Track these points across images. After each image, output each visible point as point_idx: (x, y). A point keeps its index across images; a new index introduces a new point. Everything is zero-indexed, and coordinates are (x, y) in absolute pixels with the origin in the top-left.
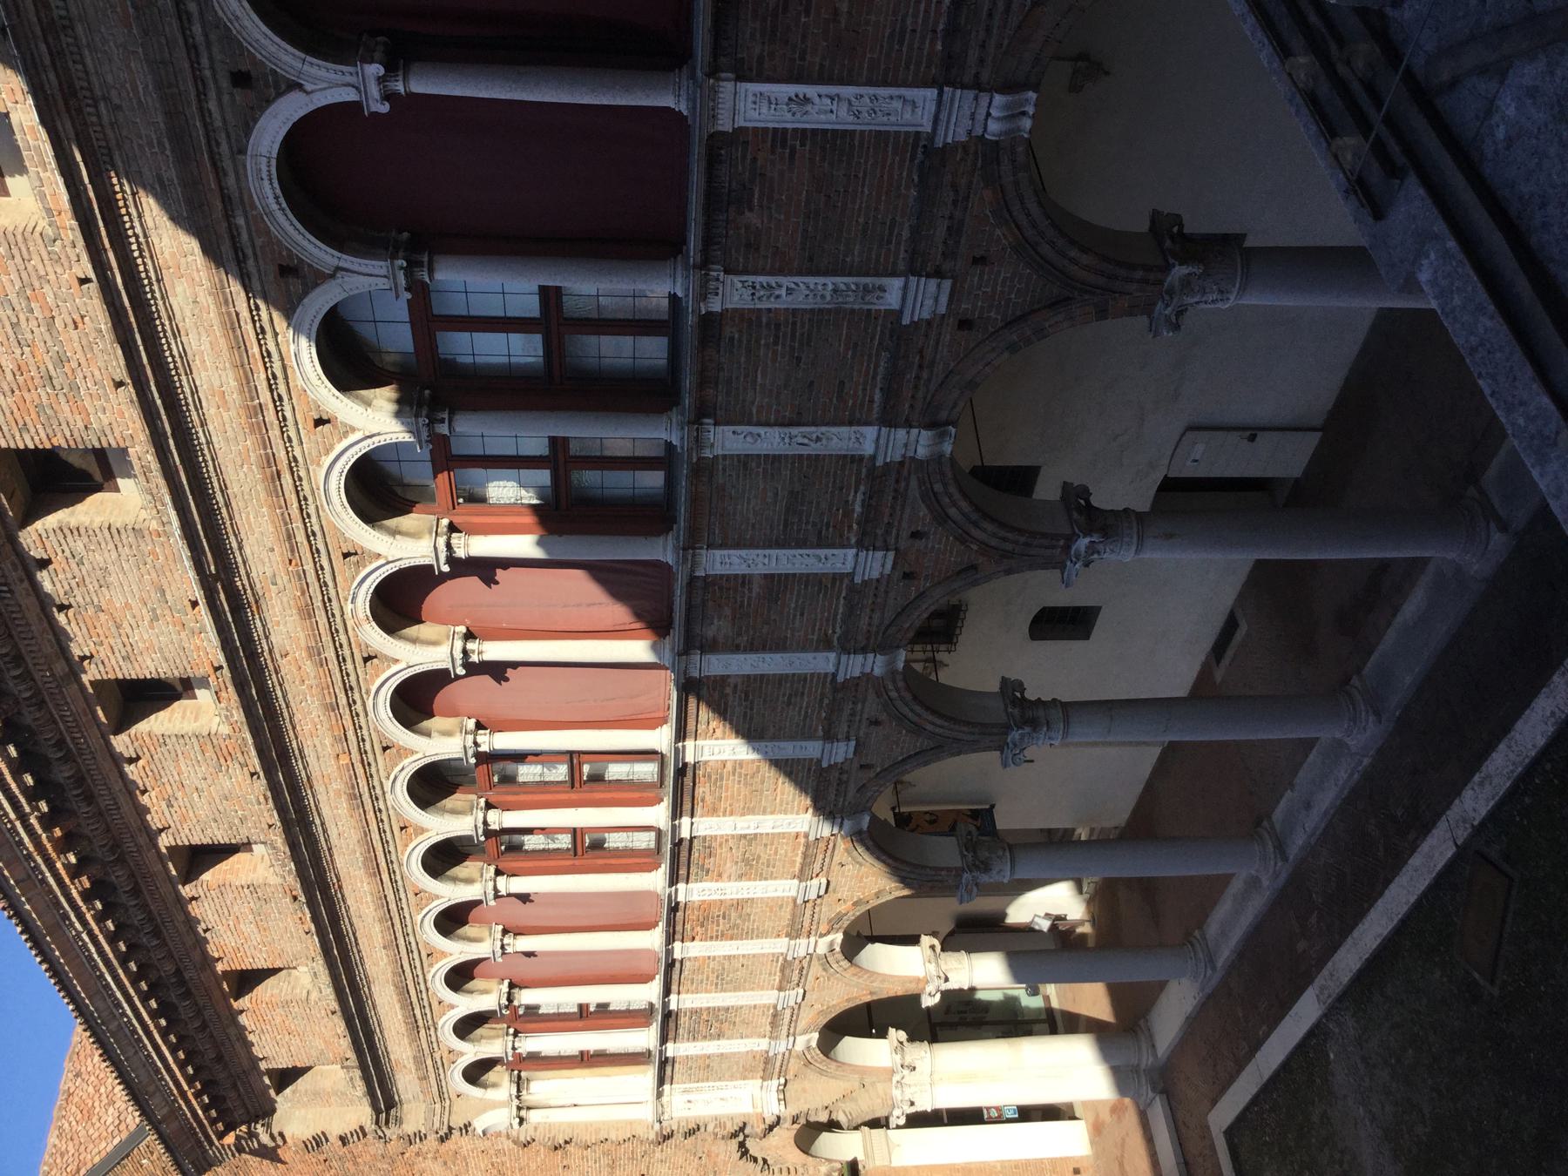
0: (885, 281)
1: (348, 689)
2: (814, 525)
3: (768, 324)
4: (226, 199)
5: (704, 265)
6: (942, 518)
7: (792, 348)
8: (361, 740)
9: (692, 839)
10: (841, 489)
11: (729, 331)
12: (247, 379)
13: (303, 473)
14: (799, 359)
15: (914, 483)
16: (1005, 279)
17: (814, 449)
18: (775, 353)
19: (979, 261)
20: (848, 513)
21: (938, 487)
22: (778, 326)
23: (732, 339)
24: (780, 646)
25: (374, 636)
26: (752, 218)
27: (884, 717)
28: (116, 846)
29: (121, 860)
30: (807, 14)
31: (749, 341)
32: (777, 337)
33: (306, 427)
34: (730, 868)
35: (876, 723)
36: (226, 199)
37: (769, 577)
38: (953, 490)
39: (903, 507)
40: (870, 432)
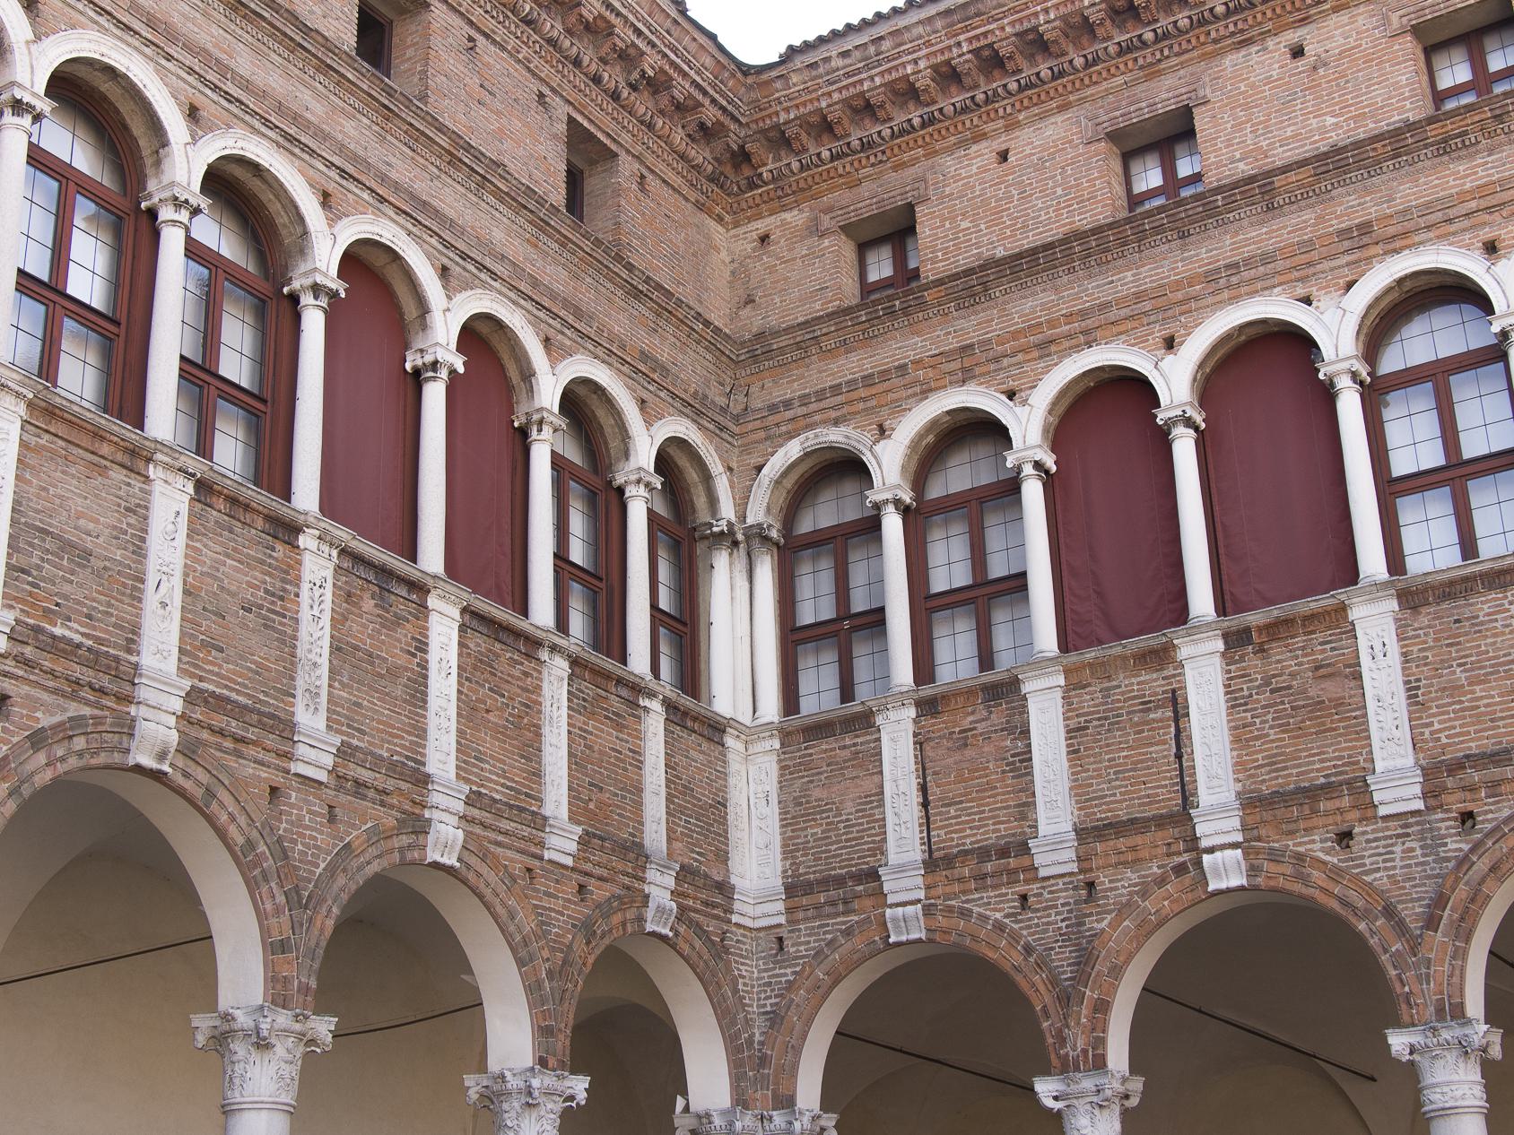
0: (323, 714)
2: (39, 568)
3: (284, 590)
4: (383, 200)
5: (344, 552)
6: (37, 739)
7: (261, 607)
10: (89, 617)
11: (281, 550)
12: (247, 85)
13: (147, 50)
14: (249, 611)
15: (87, 711)
16: (315, 839)
17: (151, 600)
18: (257, 588)
21: (80, 743)
22: (282, 599)
23: (273, 549)
26: (368, 604)
30: (490, 689)
31: (270, 565)
32: (273, 595)
33: (200, 100)
36: (383, 200)
38: (73, 762)
39: (55, 692)
40: (171, 665)
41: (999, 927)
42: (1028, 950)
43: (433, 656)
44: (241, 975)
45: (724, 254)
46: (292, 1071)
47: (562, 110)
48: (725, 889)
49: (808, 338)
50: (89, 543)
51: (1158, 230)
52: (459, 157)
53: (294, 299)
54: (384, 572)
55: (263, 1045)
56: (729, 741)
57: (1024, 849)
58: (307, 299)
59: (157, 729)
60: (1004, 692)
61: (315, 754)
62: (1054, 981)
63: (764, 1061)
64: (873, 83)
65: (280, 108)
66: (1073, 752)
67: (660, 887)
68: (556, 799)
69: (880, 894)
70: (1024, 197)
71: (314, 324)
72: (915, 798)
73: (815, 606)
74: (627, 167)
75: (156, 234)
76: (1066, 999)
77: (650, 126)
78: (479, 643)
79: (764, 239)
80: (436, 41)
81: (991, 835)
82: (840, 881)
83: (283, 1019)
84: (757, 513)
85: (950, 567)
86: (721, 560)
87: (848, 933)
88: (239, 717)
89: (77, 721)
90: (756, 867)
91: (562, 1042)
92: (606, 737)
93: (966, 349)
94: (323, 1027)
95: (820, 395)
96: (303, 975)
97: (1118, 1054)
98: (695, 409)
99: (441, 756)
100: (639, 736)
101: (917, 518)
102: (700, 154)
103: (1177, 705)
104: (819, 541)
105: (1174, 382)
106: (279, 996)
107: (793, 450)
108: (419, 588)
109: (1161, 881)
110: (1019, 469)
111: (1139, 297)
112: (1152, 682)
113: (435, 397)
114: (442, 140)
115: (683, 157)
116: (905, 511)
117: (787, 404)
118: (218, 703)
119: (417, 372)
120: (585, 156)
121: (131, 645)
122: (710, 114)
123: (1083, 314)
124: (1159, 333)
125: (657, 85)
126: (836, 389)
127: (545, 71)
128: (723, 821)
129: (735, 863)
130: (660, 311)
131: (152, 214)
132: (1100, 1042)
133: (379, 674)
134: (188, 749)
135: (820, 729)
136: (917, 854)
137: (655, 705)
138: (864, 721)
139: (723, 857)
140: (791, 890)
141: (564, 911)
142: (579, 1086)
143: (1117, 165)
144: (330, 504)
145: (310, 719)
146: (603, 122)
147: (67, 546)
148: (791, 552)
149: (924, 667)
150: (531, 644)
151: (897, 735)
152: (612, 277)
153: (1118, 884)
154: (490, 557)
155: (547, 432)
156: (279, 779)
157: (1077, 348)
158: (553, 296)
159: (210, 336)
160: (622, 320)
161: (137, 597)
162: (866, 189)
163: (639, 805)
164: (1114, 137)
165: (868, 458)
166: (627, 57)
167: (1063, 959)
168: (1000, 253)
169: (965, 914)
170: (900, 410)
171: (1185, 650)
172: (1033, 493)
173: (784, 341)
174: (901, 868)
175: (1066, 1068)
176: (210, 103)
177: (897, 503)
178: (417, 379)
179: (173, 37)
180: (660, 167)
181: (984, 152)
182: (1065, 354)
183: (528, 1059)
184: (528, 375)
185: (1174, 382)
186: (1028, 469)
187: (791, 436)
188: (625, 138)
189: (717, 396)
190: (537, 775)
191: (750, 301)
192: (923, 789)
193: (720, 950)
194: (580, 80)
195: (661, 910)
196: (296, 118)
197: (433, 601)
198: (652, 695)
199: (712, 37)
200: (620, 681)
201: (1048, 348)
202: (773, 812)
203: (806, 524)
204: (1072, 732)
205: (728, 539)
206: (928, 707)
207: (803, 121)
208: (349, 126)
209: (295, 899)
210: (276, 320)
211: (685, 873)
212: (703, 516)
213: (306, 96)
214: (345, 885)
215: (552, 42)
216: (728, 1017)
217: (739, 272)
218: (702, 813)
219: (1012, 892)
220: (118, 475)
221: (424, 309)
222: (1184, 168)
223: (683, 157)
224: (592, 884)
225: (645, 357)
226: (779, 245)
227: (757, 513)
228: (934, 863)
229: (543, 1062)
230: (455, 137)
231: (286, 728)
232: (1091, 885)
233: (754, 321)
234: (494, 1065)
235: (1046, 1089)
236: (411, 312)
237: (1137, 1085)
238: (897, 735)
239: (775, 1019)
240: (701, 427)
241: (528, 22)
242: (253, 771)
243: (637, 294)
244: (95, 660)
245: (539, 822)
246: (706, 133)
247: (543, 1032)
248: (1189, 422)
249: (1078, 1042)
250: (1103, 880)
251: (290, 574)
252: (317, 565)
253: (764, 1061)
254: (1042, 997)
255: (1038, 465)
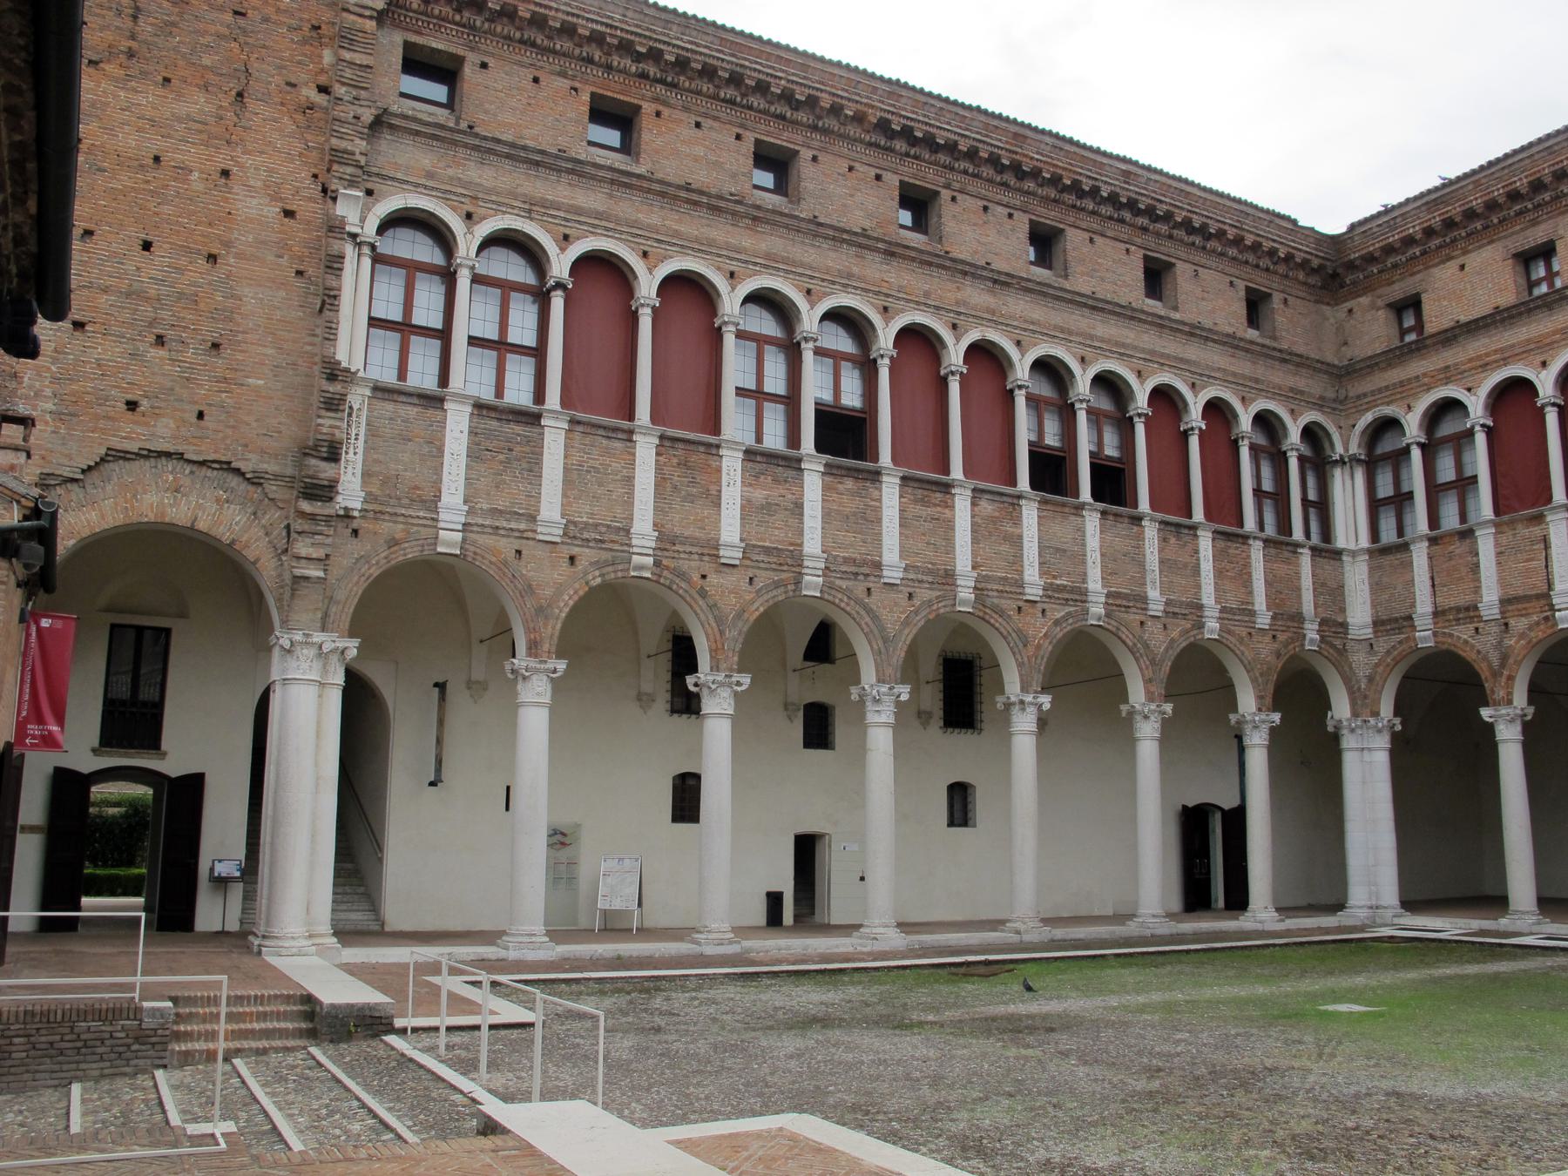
1: (937, 308)
5: (1161, 522)
6: (1057, 623)
8: (899, 299)
9: (801, 470)
19: (1165, 627)
20: (1055, 577)
24: (975, 541)
25: (973, 336)
26: (1173, 540)
27: (917, 602)
28: (826, 131)
29: (815, 128)
34: (759, 495)
35: (910, 596)
37: (1020, 537)
41: (1466, 642)
42: (1479, 652)
43: (1201, 555)
44: (1137, 693)
45: (1332, 320)
46: (1157, 725)
47: (1241, 285)
48: (1344, 625)
49: (1374, 364)
50: (1065, 547)
51: (1536, 308)
52: (1194, 332)
53: (1131, 418)
54: (1178, 525)
55: (1146, 717)
56: (1345, 558)
57: (1476, 608)
58: (1136, 419)
59: (1097, 609)
60: (1467, 534)
61: (1156, 606)
62: (1490, 666)
63: (1366, 697)
64: (1394, 238)
65: (1117, 344)
66: (1499, 563)
67: (1312, 633)
68: (1260, 602)
69: (1413, 627)
70: (1473, 290)
71: (1140, 430)
72: (1428, 583)
73: (1385, 489)
74: (1277, 298)
75: (1075, 414)
76: (1496, 674)
77: (1286, 276)
78: (1221, 544)
79: (1350, 311)
80: (1180, 280)
81: (1463, 600)
82: (1396, 620)
83: (1153, 707)
84: (1354, 448)
85: (1446, 470)
86: (1337, 472)
87: (1400, 642)
88: (1126, 600)
89: (1069, 614)
90: (1359, 614)
91: (1269, 700)
92: (1281, 569)
93: (1447, 367)
94: (1168, 708)
95: (1380, 390)
96: (1159, 690)
97: (1520, 698)
98: (1320, 404)
99: (1208, 596)
100: (1298, 565)
101: (1429, 450)
102: (1312, 280)
103: (1546, 541)
104: (1386, 457)
105: (1546, 385)
106: (1150, 698)
107: (1369, 417)
108: (1194, 528)
109: (1538, 624)
110: (1473, 427)
111: (1528, 341)
112: (1536, 531)
113: (1194, 442)
114: (1187, 329)
115: (1305, 284)
116: (1422, 446)
117: (1365, 395)
118: (1117, 595)
119: (1186, 432)
120: (1255, 305)
121: (1084, 581)
122: (1315, 263)
123: (1501, 350)
124: (1540, 359)
125: (1289, 258)
126: (1387, 388)
127: (1232, 271)
128: (1343, 594)
129: (1348, 612)
130: (1298, 365)
131: (1072, 405)
132: (1510, 694)
133: (1181, 568)
134: (1108, 615)
135: (1386, 550)
136: (1429, 609)
137: (1306, 551)
138: (1404, 547)
139: (1343, 610)
140: (1377, 624)
141: (1265, 649)
142: (1276, 717)
143: (1520, 269)
144: (1153, 506)
145: (1153, 593)
146: (1261, 282)
147: (1058, 550)
148: (1371, 465)
149: (1434, 522)
150: (1245, 538)
151: (1420, 555)
152: (1273, 358)
153: (1519, 624)
154: (1224, 506)
155: (1246, 442)
156: (1143, 618)
157: (1499, 367)
158: (1244, 377)
159: (1100, 443)
160: (1280, 377)
161: (1084, 562)
162: (1396, 287)
163: (1299, 597)
164: (1517, 256)
165: (1403, 421)
166: (1272, 253)
167: (1495, 659)
168: (1463, 319)
169: (1451, 635)
170: (1415, 396)
171: (1549, 519)
172: (1480, 439)
173: (1362, 365)
174: (1423, 615)
175: (1496, 704)
176: (1088, 352)
177: (1419, 444)
178: (1185, 435)
179: (1070, 333)
180: (1294, 292)
181: (1452, 266)
182: (1494, 370)
183: (1254, 709)
184: (1235, 416)
185: (1546, 385)
186: (1477, 428)
187: (1367, 410)
188: (1275, 285)
189: (1330, 394)
190: (1251, 593)
191: (1346, 343)
192: (1432, 578)
193: (1343, 652)
194: (1249, 269)
195: (1312, 640)
196: (1123, 345)
197: (1199, 533)
198: (1303, 546)
199: (1312, 229)
200: (1288, 544)
201: (1486, 367)
202: (1366, 588)
203: (1379, 451)
204: (1499, 554)
205: (1341, 462)
206: (1433, 541)
207: (1362, 258)
208: (1146, 337)
209: (1153, 662)
210: (1125, 426)
211: (1323, 622)
212: (1328, 452)
213: (1126, 332)
214: (1173, 654)
215: (1234, 259)
216: (1348, 681)
217: (1340, 328)
218: (1332, 593)
219: (1471, 626)
220: (1072, 518)
221: (1186, 404)
222: (1556, 268)
223: (1305, 284)
224: (1279, 635)
225: (1292, 390)
226: (1358, 314)
227: (1354, 448)
228: (1436, 614)
229: (1260, 710)
230: (1192, 326)
231: (1143, 599)
232: (1506, 624)
233: (1348, 352)
234: (1241, 710)
235: (1485, 713)
236: (1181, 405)
237: (1531, 710)
238: (1420, 555)
239: (1371, 679)
240: (1323, 413)
241: (1222, 254)
242: (1133, 617)
243: (1284, 361)
244: (1072, 590)
245: (1252, 613)
246: (1314, 271)
247: (1260, 698)
248: (1554, 405)
249: (1501, 693)
250: (1512, 622)
251: (1140, 537)
252: (1151, 531)
253: (1366, 697)
254: (1485, 673)
255: (1483, 426)
